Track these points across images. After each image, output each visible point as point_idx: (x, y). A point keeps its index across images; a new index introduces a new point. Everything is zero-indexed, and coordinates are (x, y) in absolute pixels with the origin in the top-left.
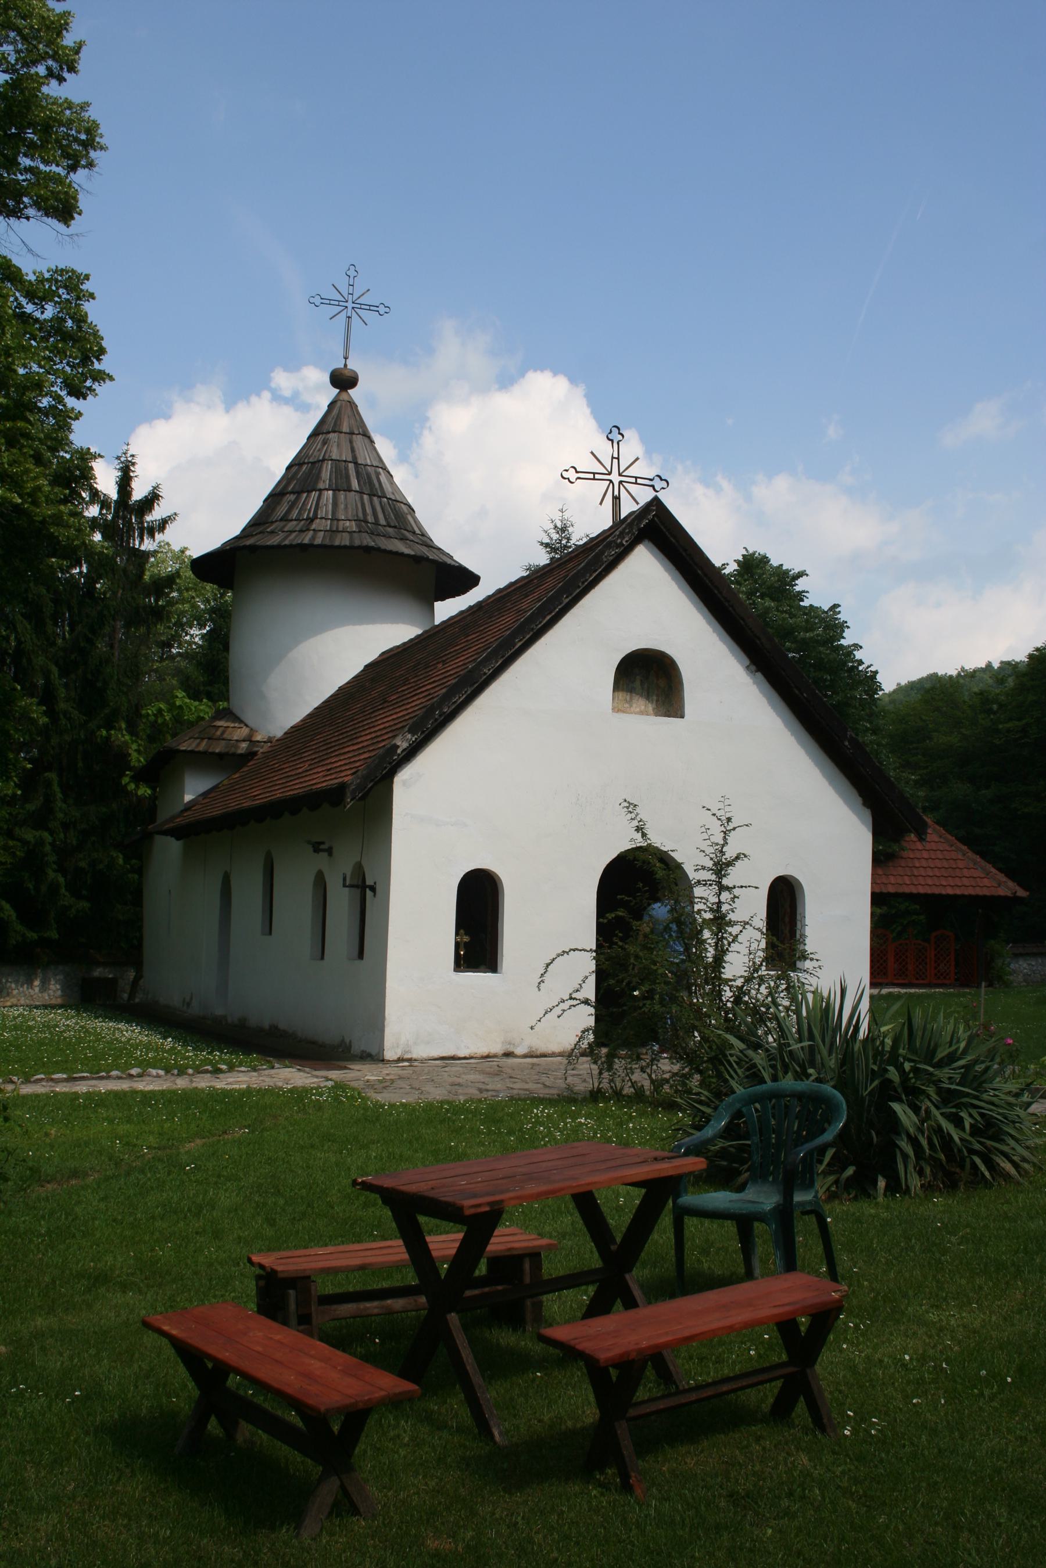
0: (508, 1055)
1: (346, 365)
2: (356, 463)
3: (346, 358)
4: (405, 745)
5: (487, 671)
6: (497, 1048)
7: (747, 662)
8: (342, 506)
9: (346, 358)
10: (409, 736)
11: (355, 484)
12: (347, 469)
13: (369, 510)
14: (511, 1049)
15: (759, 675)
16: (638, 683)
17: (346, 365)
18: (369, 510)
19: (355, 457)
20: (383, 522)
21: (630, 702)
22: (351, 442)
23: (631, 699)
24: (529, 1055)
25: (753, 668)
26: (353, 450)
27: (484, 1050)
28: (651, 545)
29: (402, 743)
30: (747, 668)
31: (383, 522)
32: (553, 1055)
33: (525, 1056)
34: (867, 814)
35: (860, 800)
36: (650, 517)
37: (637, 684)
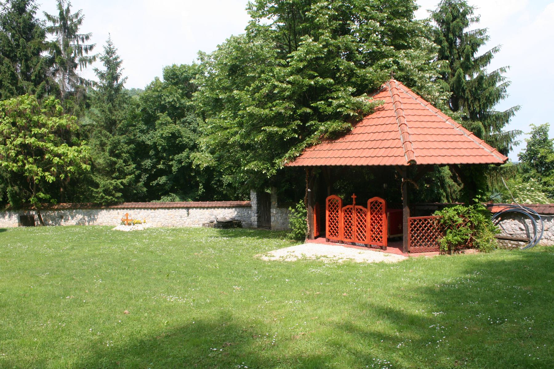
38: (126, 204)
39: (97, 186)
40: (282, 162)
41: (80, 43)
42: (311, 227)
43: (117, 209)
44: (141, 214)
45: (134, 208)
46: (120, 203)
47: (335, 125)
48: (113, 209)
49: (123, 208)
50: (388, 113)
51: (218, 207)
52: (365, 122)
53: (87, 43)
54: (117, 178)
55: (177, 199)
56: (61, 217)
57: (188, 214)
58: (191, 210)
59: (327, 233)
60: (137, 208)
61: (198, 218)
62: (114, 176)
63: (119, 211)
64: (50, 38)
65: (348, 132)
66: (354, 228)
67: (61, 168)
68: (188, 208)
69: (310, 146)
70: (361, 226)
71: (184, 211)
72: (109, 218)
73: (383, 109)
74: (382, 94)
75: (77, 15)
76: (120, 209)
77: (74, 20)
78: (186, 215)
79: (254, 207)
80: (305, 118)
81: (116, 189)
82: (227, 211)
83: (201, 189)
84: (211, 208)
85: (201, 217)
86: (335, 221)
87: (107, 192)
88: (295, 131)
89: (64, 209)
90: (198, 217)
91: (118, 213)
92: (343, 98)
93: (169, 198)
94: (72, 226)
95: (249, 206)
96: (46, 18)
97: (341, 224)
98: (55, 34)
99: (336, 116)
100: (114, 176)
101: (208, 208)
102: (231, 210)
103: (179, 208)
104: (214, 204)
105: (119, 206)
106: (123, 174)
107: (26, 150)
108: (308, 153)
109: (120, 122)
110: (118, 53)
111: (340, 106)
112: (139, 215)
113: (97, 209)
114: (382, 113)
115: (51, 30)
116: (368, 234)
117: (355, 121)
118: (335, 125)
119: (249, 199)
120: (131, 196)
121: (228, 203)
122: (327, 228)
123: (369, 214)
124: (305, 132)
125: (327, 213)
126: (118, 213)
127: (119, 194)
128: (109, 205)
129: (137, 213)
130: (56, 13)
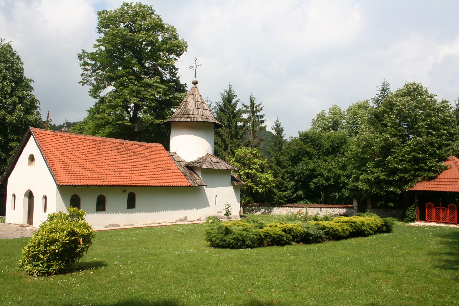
38: (288, 205)
39: (275, 194)
40: (407, 188)
41: (259, 119)
42: (418, 217)
43: (283, 207)
45: (292, 207)
46: (286, 204)
47: (431, 175)
48: (281, 207)
49: (287, 207)
50: (454, 170)
51: (337, 208)
52: (443, 173)
53: (262, 119)
54: (284, 191)
55: (308, 202)
56: (253, 210)
58: (322, 209)
59: (426, 218)
60: (294, 207)
62: (282, 189)
64: (245, 116)
65: (436, 177)
66: (441, 216)
67: (264, 185)
68: (321, 208)
69: (418, 182)
70: (445, 216)
71: (319, 209)
72: (278, 211)
73: (450, 168)
74: (447, 162)
75: (259, 105)
77: (258, 108)
79: (356, 208)
80: (416, 170)
81: (285, 197)
82: (341, 209)
83: (322, 198)
84: (333, 208)
86: (430, 213)
87: (280, 198)
88: (412, 176)
89: (255, 206)
92: (431, 163)
93: (303, 202)
94: (258, 216)
95: (352, 208)
96: (242, 106)
97: (434, 214)
98: (247, 114)
99: (430, 169)
100: (282, 189)
101: (331, 208)
102: (343, 209)
103: (316, 207)
104: (335, 206)
105: (285, 205)
106: (287, 189)
107: (248, 176)
108: (418, 185)
109: (285, 161)
110: (282, 126)
111: (432, 166)
113: (272, 206)
114: (451, 170)
115: (244, 112)
116: (448, 218)
117: (439, 173)
118: (431, 175)
119: (352, 204)
120: (291, 201)
121: (341, 206)
122: (426, 216)
123: (448, 210)
124: (415, 176)
125: (426, 210)
127: (286, 199)
128: (280, 205)
130: (249, 104)
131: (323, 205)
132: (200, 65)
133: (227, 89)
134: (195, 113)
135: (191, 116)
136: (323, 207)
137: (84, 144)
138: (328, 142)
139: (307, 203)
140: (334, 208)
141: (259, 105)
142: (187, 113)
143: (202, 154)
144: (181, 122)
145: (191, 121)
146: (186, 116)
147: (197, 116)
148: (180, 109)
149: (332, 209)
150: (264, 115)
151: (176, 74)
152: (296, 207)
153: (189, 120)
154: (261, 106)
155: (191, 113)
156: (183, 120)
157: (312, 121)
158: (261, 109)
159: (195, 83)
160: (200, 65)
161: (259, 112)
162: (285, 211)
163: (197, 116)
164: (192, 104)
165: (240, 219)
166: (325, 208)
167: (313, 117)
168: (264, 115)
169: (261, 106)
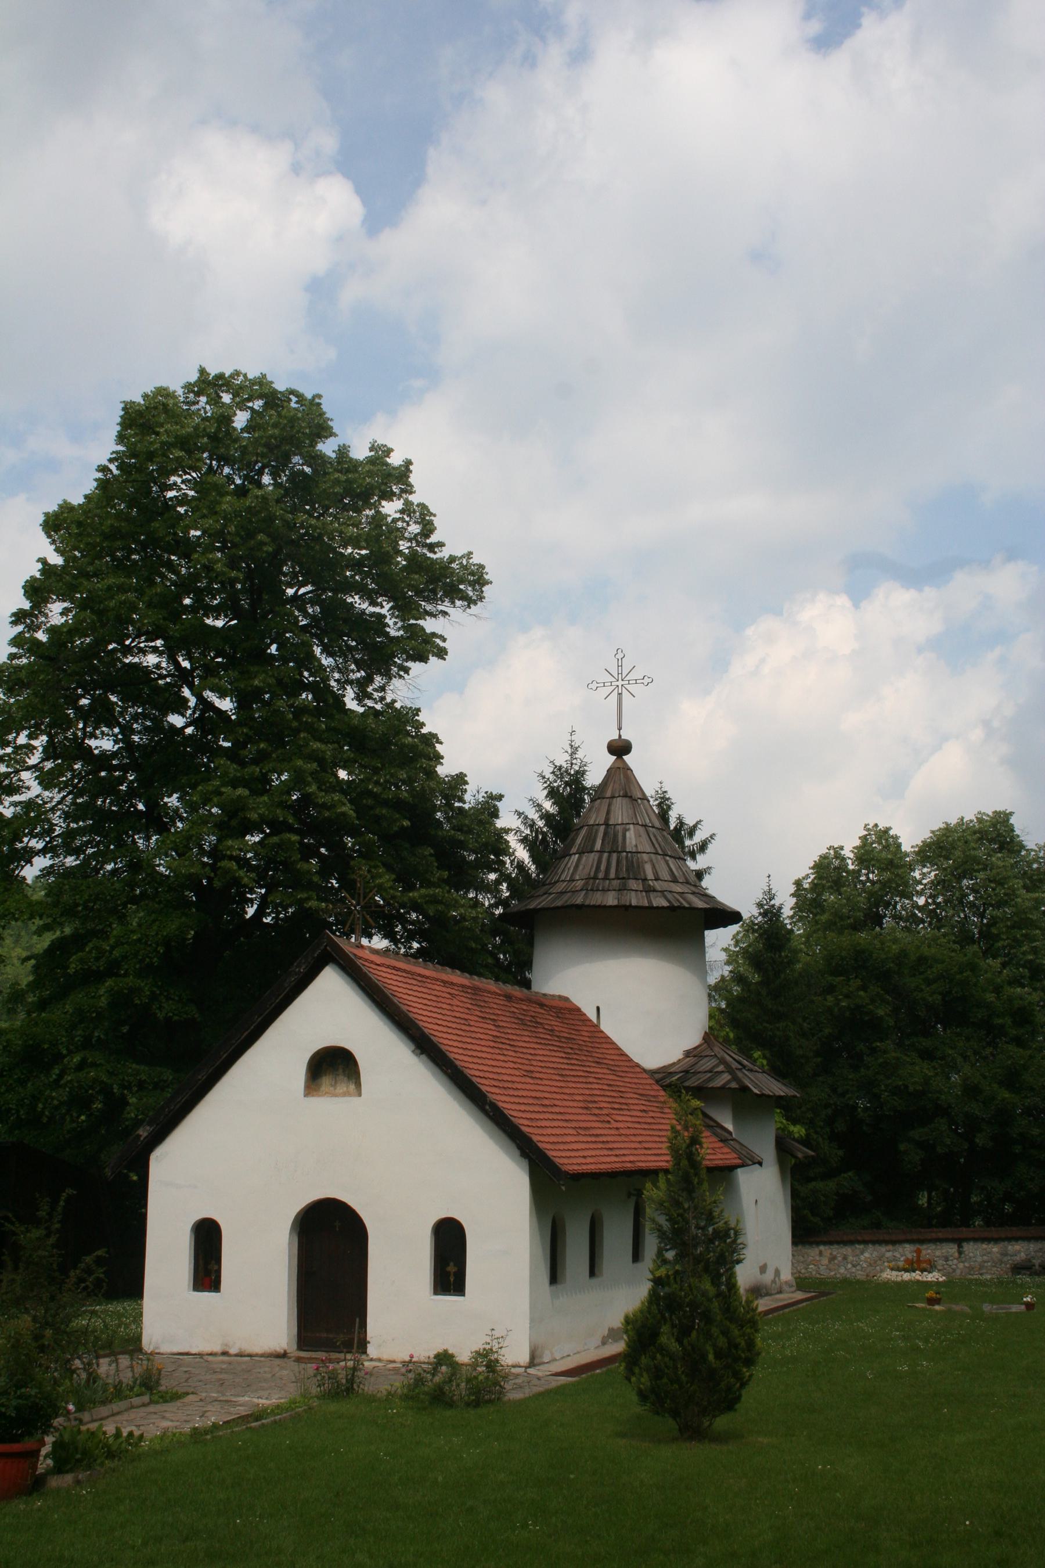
0: (225, 1353)
1: (620, 736)
2: (607, 824)
3: (620, 729)
4: (145, 1134)
5: (202, 1077)
6: (217, 1349)
7: (413, 1047)
8: (581, 867)
9: (620, 729)
10: (148, 1128)
11: (598, 846)
12: (597, 831)
13: (603, 867)
14: (227, 1349)
15: (424, 1057)
16: (341, 1071)
17: (620, 736)
18: (603, 867)
19: (607, 819)
20: (612, 875)
21: (334, 1086)
22: (609, 805)
23: (336, 1083)
24: (240, 1355)
25: (418, 1051)
26: (608, 813)
27: (208, 1349)
28: (334, 966)
29: (143, 1132)
30: (413, 1052)
31: (612, 875)
32: (257, 1355)
33: (236, 1355)
34: (525, 1163)
35: (517, 1152)
36: (322, 948)
37: (341, 1071)
43: (818, 1243)
44: (867, 1255)
45: (851, 1243)
48: (811, 1243)
51: (1016, 1239)
57: (960, 1253)
58: (965, 1244)
60: (859, 1242)
61: (984, 1258)
63: (822, 1248)
68: (959, 1242)
71: (951, 1249)
76: (825, 1243)
77: (688, 843)
78: (956, 1254)
82: (1033, 1247)
85: (985, 1258)
90: (979, 1259)
91: (821, 1253)
101: (996, 1240)
112: (862, 1257)
126: (821, 1253)
129: (858, 1252)
131: (964, 1232)
132: (647, 681)
133: (562, 760)
134: (665, 874)
135: (658, 885)
136: (968, 1240)
137: (455, 1002)
138: (929, 982)
139: (878, 1226)
140: (1009, 1239)
141: (691, 833)
142: (631, 869)
143: (692, 1038)
144: (628, 908)
145: (672, 908)
146: (633, 884)
147: (678, 888)
148: (593, 857)
149: (1002, 1244)
150: (708, 870)
151: (382, 689)
152: (865, 1242)
153: (665, 904)
154: (699, 837)
155: (650, 875)
156: (635, 899)
157: (792, 889)
158: (703, 847)
159: (620, 749)
160: (647, 681)
161: (693, 857)
162: (825, 1261)
163: (678, 888)
164: (638, 835)
165: (800, 1295)
166: (975, 1240)
167: (800, 875)
168: (708, 870)
169: (699, 837)
